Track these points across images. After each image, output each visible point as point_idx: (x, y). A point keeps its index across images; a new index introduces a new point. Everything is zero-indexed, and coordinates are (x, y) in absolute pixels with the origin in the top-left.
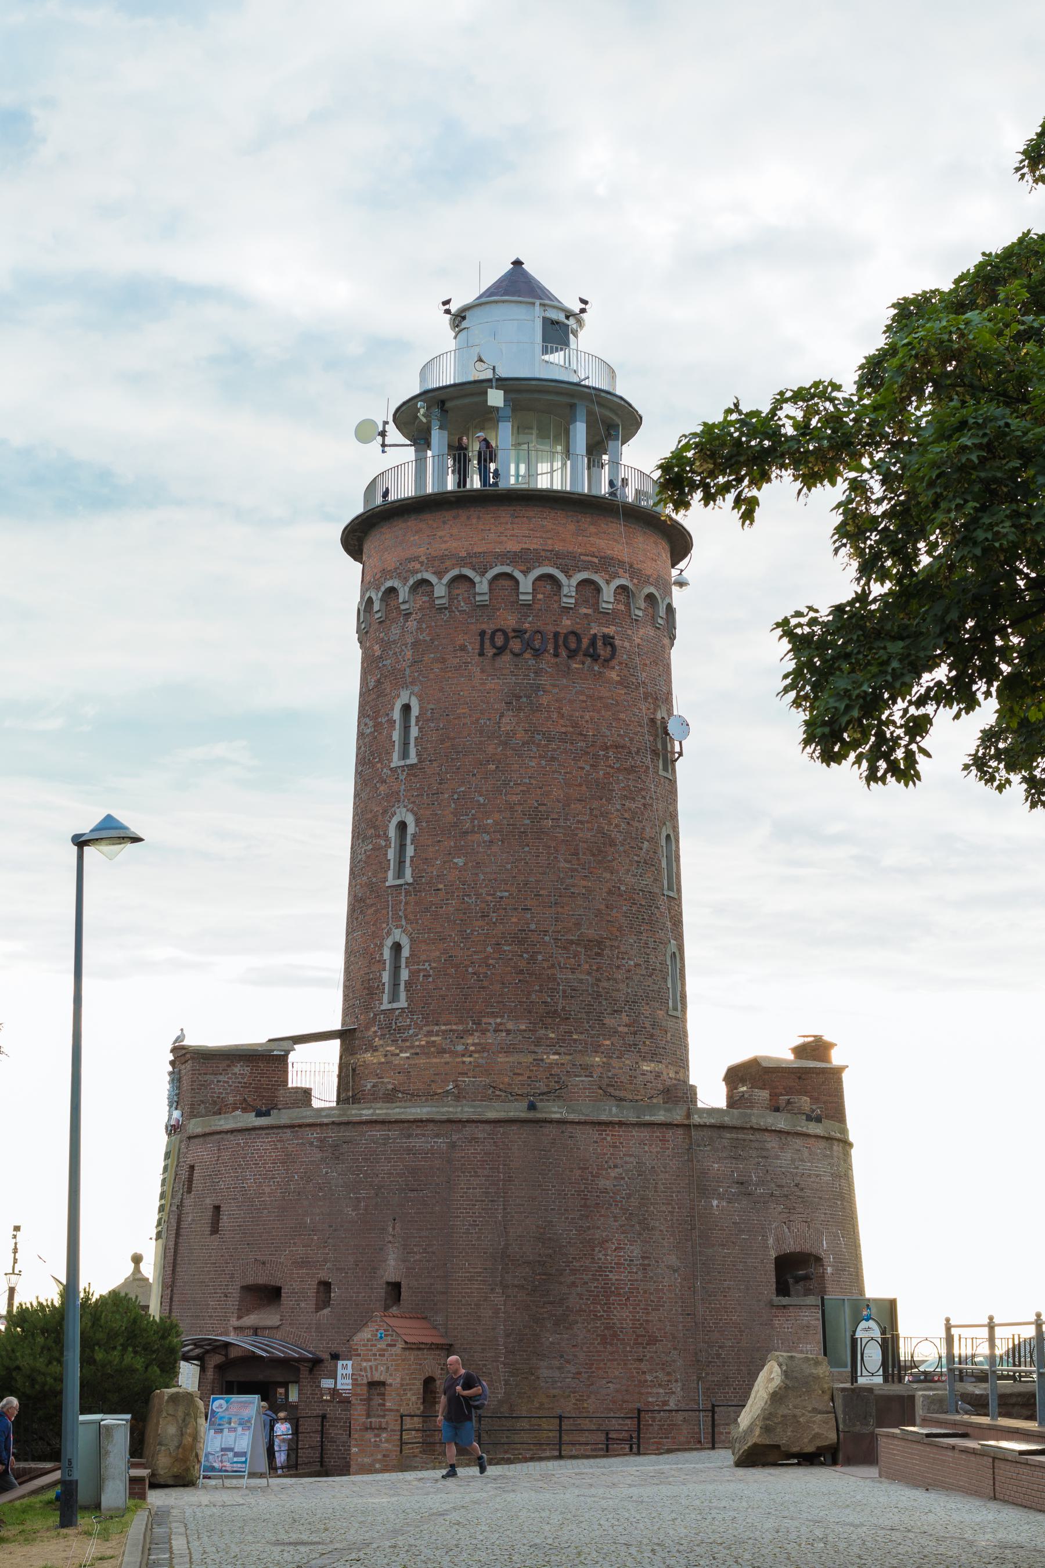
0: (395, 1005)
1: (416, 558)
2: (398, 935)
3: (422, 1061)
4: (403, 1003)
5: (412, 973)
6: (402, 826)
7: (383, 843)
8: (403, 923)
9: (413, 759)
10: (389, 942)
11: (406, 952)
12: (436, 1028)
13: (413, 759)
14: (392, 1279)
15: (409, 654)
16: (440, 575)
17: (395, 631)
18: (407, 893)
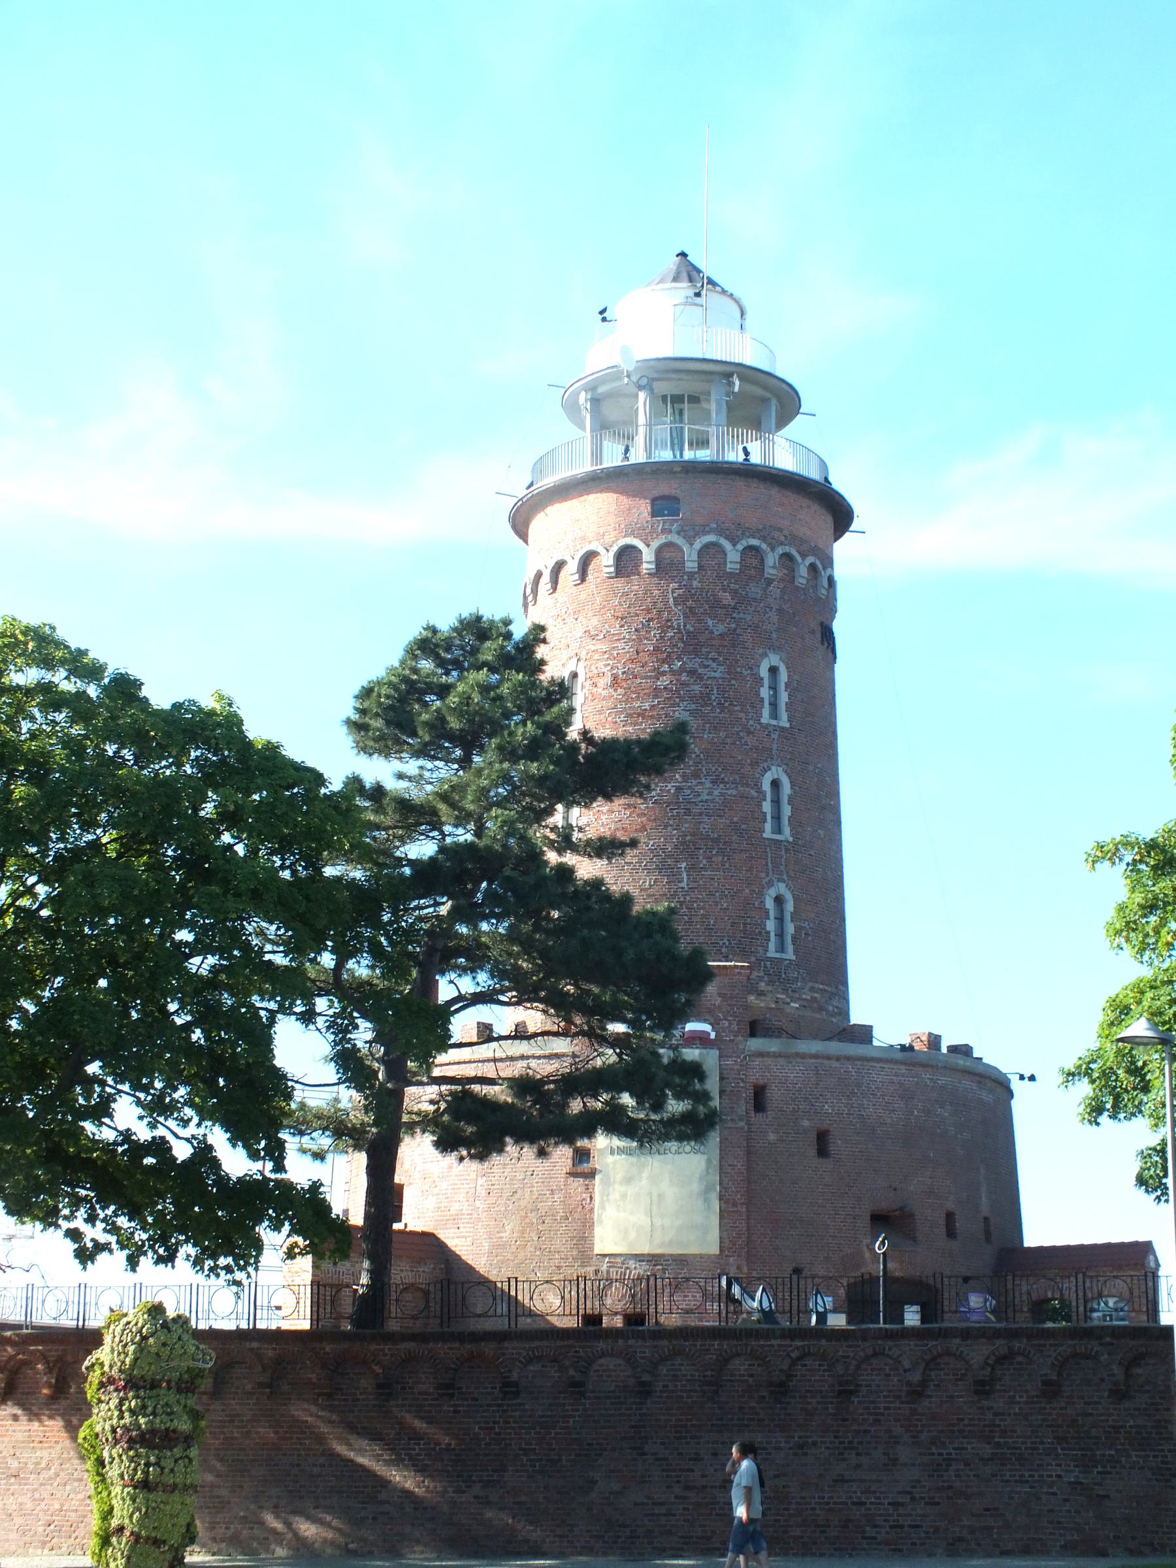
0: (784, 956)
1: (781, 530)
2: (782, 888)
3: (808, 1013)
4: (790, 954)
5: (798, 929)
6: (775, 784)
7: (755, 794)
8: (785, 877)
9: (784, 722)
10: (772, 892)
11: (790, 907)
12: (816, 986)
13: (784, 722)
14: (987, 1215)
15: (775, 619)
16: (804, 556)
17: (755, 590)
18: (787, 850)
